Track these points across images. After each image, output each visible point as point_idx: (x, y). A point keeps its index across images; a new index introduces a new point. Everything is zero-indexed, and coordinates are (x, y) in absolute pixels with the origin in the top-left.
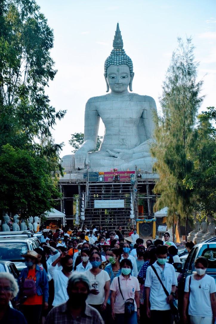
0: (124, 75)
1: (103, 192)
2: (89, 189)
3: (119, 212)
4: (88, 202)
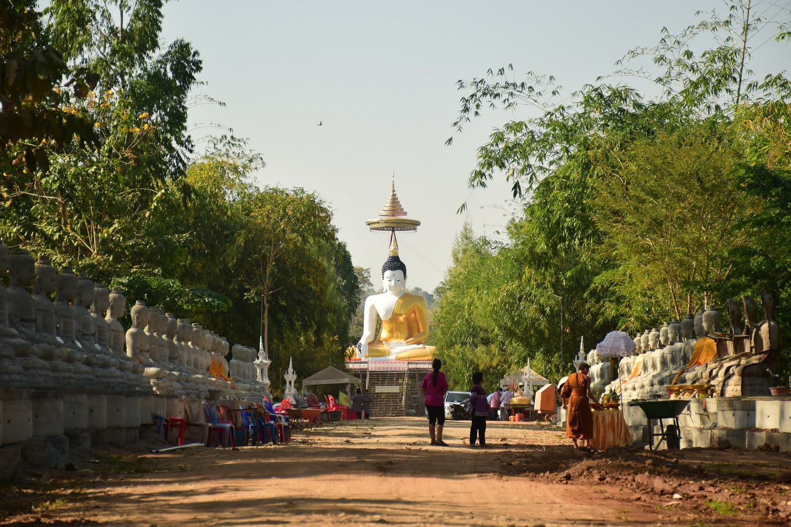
1: (380, 379)
3: (393, 396)
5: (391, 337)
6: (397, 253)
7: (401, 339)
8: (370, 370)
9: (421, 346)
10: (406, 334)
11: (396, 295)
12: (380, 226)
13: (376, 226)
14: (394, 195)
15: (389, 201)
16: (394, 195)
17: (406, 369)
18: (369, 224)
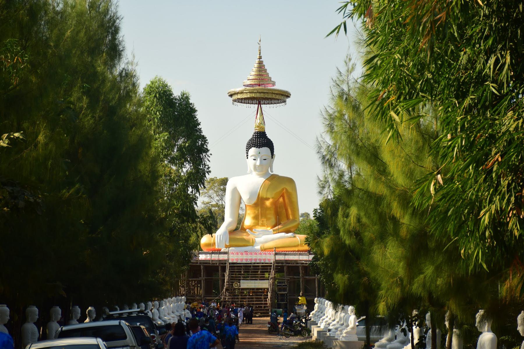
1: (242, 273)
2: (229, 269)
3: (257, 292)
5: (257, 224)
6: (264, 128)
7: (268, 227)
8: (230, 261)
9: (290, 234)
10: (273, 221)
11: (262, 176)
12: (244, 96)
13: (240, 96)
14: (261, 63)
15: (255, 69)
16: (261, 63)
17: (272, 261)
18: (231, 96)
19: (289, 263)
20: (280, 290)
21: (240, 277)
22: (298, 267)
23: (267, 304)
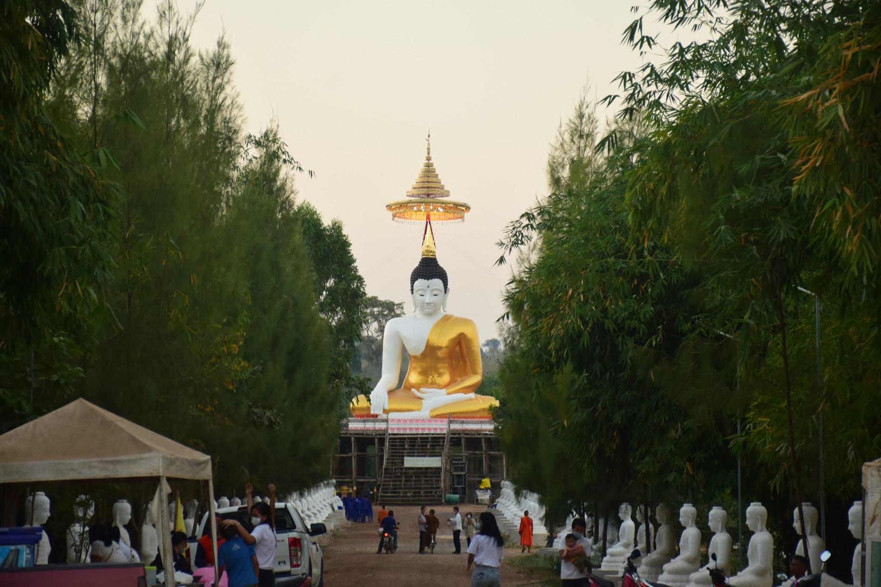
0: (436, 292)
1: (406, 447)
2: (389, 442)
3: (426, 473)
4: (388, 459)
8: (390, 432)
14: (429, 165)
16: (429, 165)
19: (468, 434)
20: (456, 469)
21: (403, 453)
22: (480, 438)
23: (439, 488)
